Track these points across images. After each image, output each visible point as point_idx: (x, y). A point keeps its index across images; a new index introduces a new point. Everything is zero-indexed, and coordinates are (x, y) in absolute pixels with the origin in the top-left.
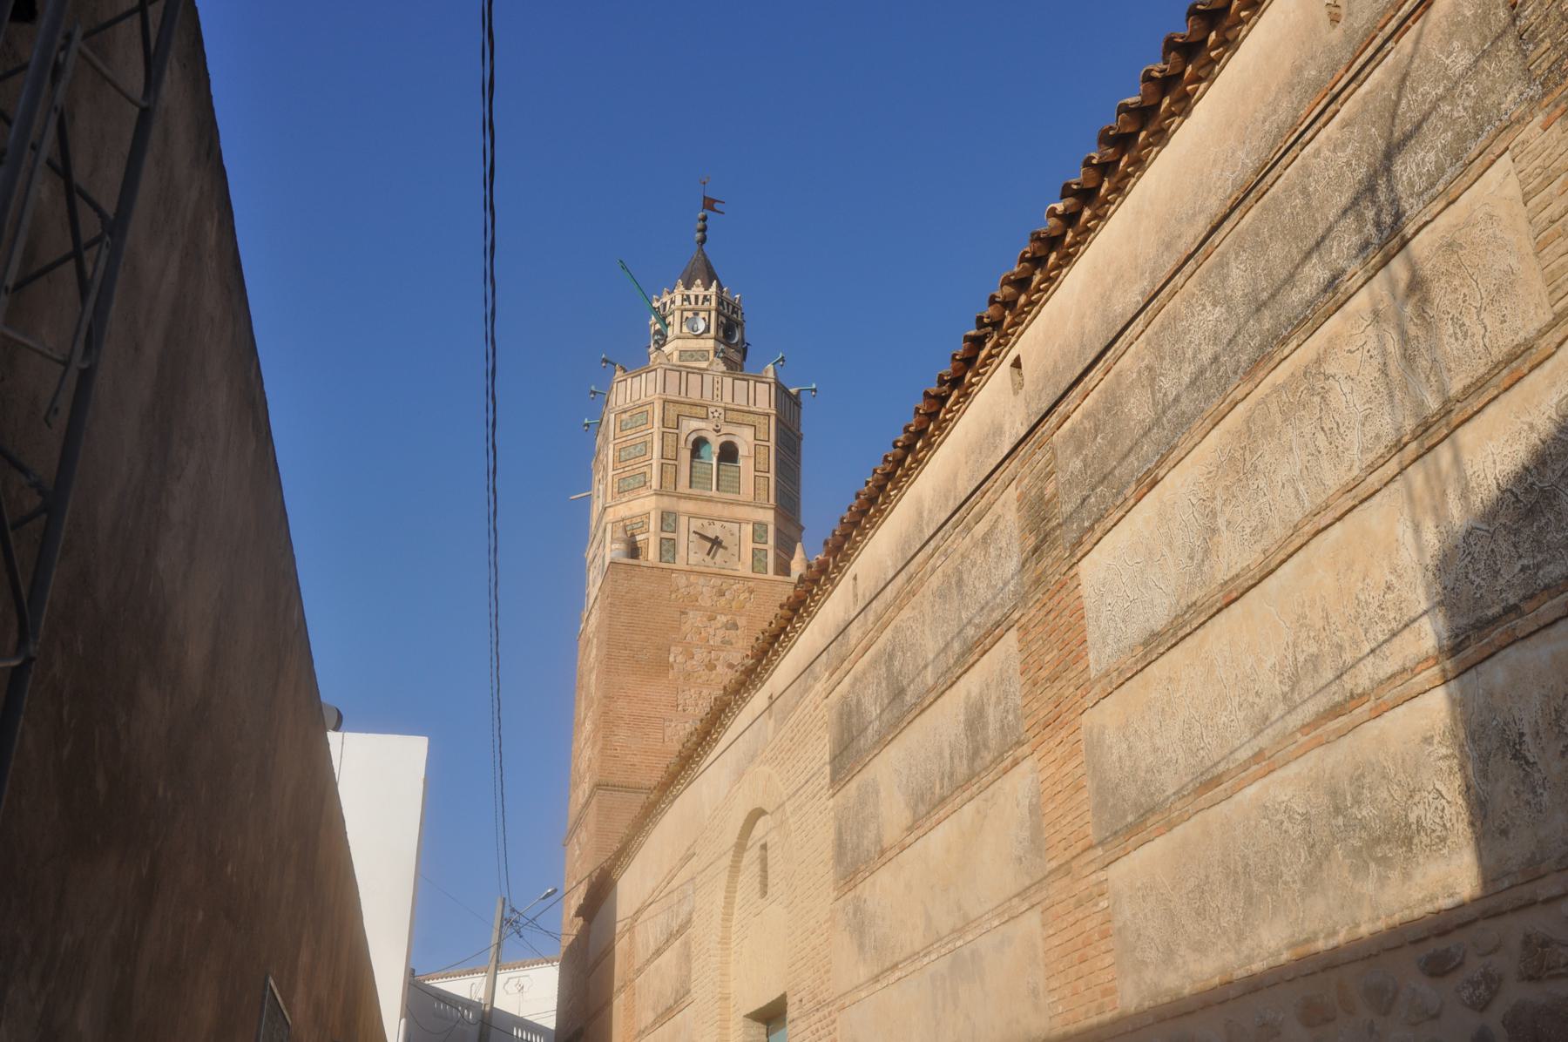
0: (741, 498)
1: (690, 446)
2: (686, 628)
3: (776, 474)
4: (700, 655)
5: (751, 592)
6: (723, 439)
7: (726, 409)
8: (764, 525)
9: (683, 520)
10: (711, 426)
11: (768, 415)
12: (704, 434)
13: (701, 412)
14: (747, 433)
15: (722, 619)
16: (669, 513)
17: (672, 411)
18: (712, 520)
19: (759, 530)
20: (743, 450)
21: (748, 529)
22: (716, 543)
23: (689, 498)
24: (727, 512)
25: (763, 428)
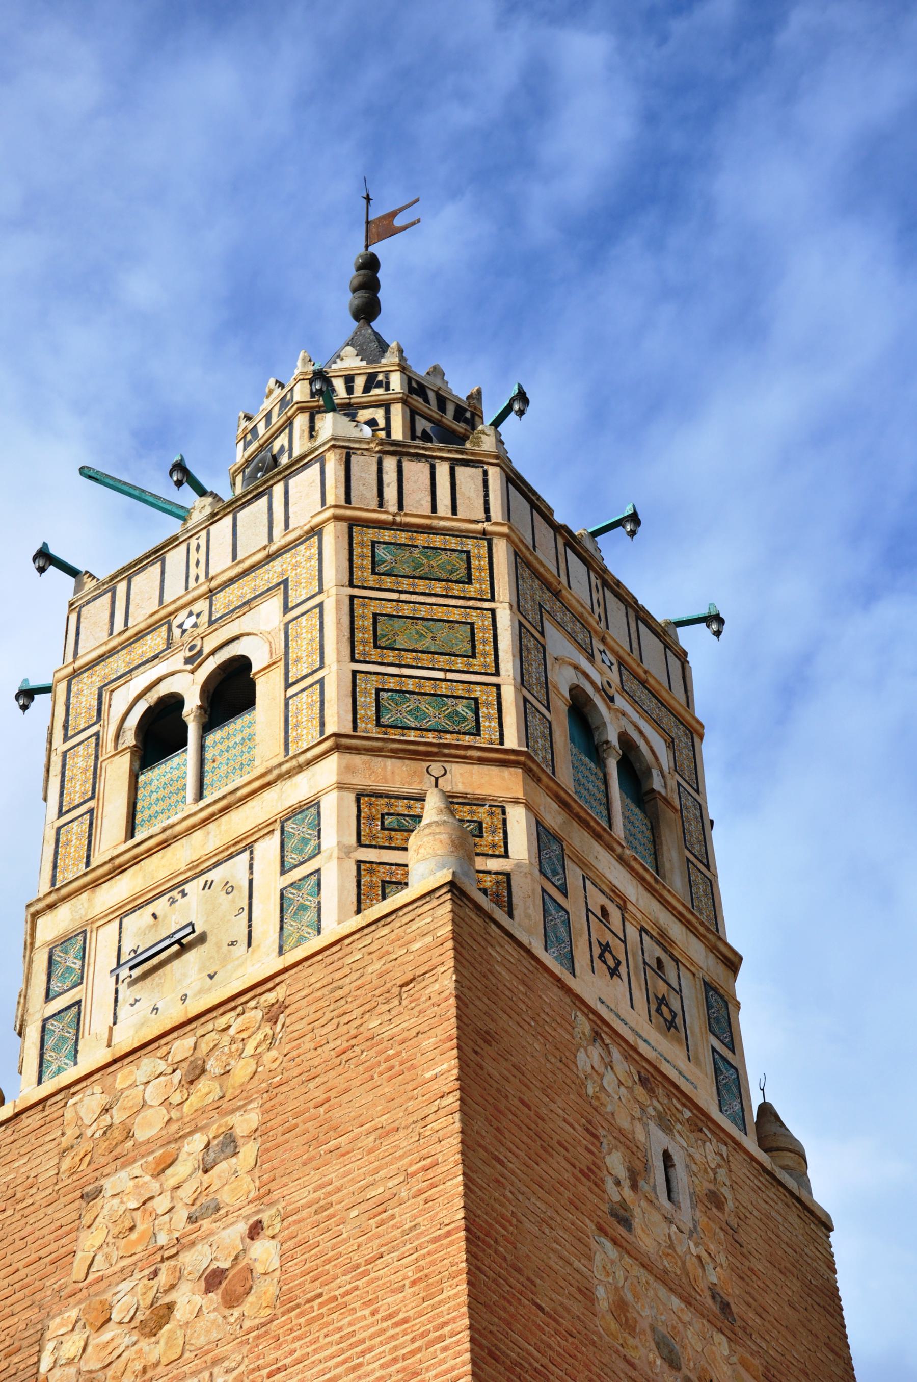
1: (129, 739)
2: (89, 1241)
4: (128, 1298)
5: (273, 1015)
6: (210, 665)
8: (310, 808)
10: (177, 661)
11: (316, 532)
12: (163, 689)
13: (155, 642)
14: (269, 614)
15: (197, 1142)
16: (65, 941)
18: (176, 887)
19: (296, 827)
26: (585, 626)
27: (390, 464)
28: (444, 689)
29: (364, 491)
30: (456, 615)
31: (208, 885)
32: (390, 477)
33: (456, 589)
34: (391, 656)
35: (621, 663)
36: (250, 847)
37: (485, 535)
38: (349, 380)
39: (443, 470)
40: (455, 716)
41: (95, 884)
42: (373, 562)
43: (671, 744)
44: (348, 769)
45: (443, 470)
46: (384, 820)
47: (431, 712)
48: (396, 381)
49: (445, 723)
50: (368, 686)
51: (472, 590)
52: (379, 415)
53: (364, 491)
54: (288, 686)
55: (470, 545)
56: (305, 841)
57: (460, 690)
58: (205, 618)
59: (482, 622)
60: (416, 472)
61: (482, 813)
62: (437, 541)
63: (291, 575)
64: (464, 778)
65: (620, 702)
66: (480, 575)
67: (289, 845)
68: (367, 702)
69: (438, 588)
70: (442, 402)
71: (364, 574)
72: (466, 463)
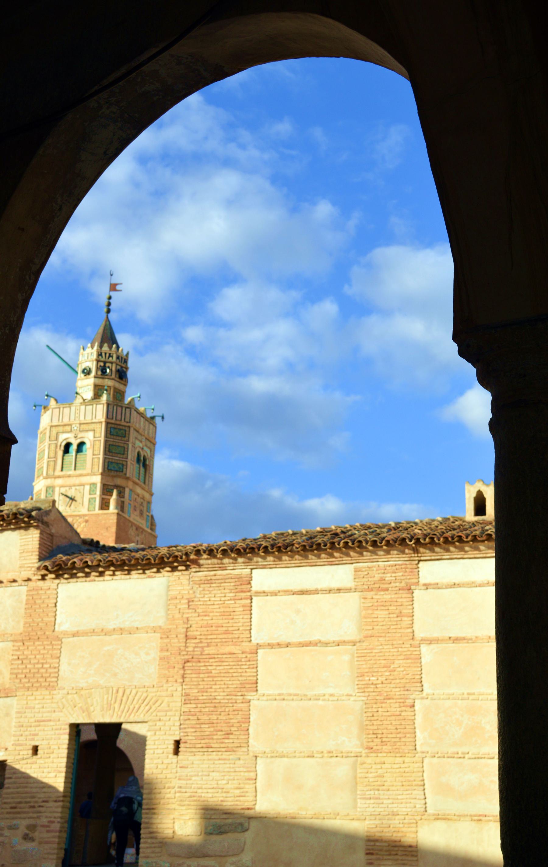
0: (84, 472)
1: (62, 448)
3: (105, 453)
6: (79, 441)
7: (80, 424)
9: (57, 490)
11: (101, 422)
13: (68, 428)
17: (54, 431)
18: (70, 487)
20: (88, 446)
21: (87, 488)
22: (72, 499)
23: (59, 477)
24: (77, 481)
25: (98, 430)
26: (141, 435)
27: (115, 408)
28: (119, 462)
29: (110, 414)
30: (122, 445)
31: (76, 489)
32: (115, 411)
33: (123, 439)
34: (111, 454)
35: (146, 439)
36: (84, 486)
37: (129, 427)
38: (106, 354)
39: (124, 409)
40: (120, 468)
41: (55, 478)
42: (111, 432)
43: (151, 451)
44: (102, 479)
45: (124, 409)
46: (106, 490)
47: (116, 466)
48: (115, 356)
49: (118, 470)
50: (107, 461)
51: (126, 439)
52: (110, 365)
53: (110, 414)
54: (93, 455)
55: (127, 429)
56: (94, 491)
57: (121, 462)
58: (78, 429)
59: (126, 446)
60: (119, 409)
61: (121, 489)
62: (121, 427)
63: (96, 429)
64: (119, 481)
65: (145, 448)
66: (127, 435)
67: (92, 489)
68: (106, 464)
69: (120, 438)
70: (122, 358)
71: (108, 435)
72: (128, 408)
